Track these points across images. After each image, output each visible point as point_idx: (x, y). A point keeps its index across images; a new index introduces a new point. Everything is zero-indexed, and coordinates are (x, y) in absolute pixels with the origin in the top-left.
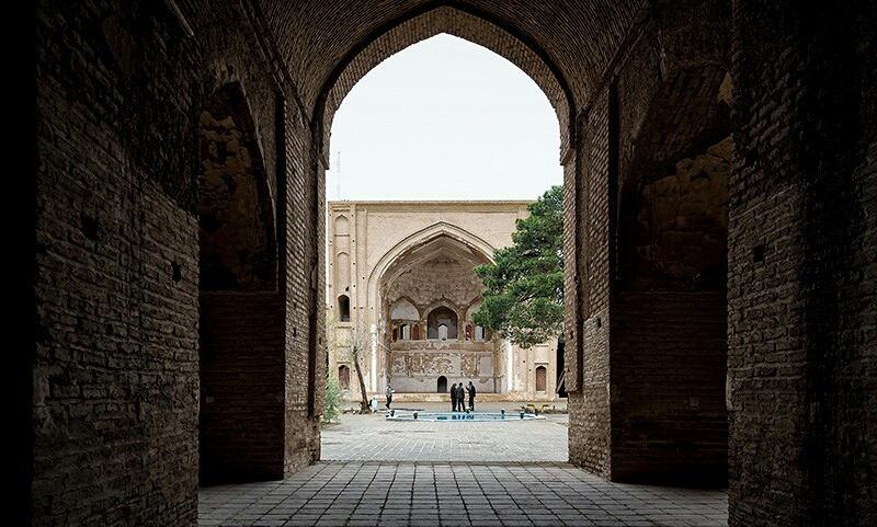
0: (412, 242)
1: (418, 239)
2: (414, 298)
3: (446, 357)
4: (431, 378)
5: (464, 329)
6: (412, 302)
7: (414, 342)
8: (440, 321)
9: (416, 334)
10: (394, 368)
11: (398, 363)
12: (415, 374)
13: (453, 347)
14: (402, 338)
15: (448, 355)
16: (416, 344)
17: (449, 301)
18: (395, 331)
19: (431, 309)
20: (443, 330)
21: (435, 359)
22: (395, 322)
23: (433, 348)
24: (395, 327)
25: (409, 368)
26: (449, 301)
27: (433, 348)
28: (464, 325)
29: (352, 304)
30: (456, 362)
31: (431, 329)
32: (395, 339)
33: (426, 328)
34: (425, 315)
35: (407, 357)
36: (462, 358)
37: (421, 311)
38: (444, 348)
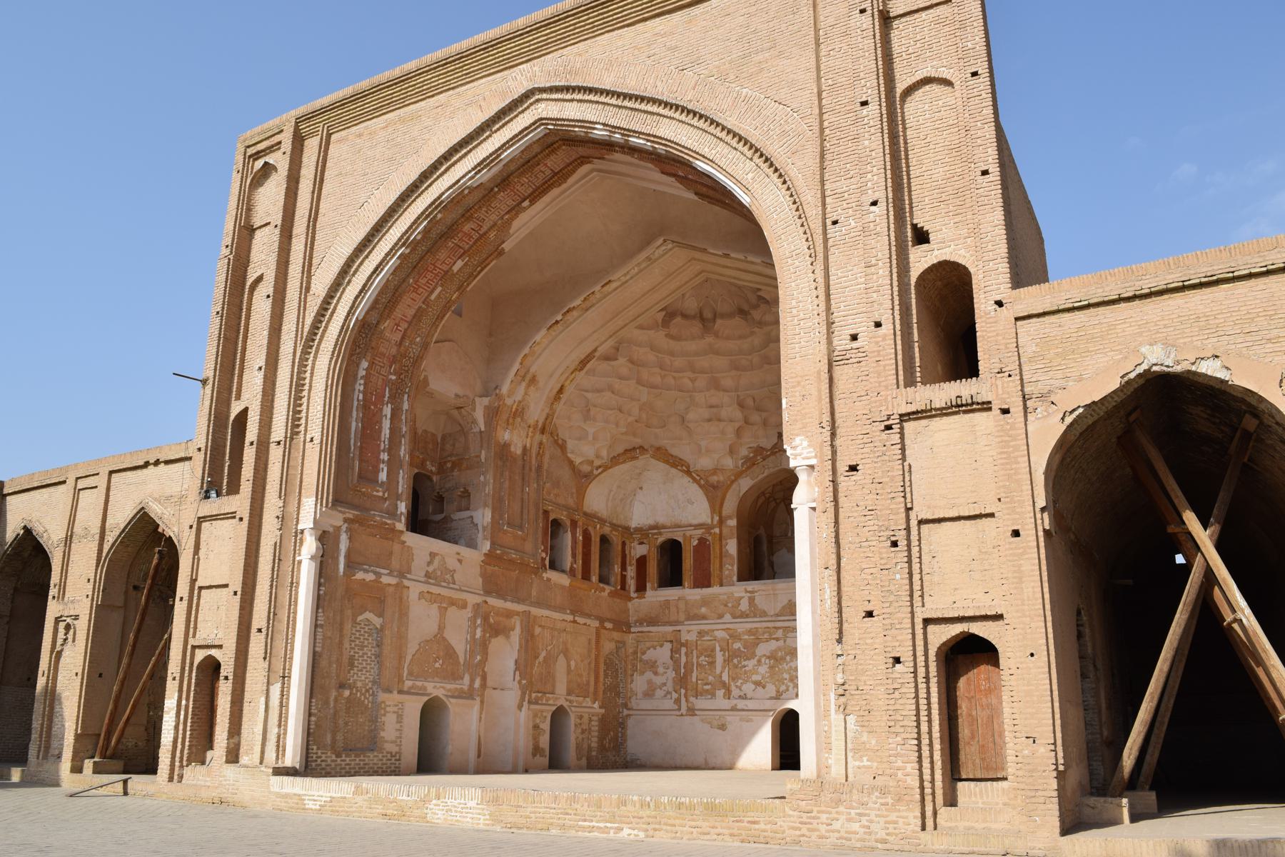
10: (639, 683)
11: (652, 666)
12: (700, 703)
16: (705, 602)
18: (642, 562)
19: (745, 484)
21: (763, 649)
22: (644, 534)
23: (754, 611)
24: (639, 550)
25: (682, 681)
27: (754, 611)
29: (252, 433)
32: (641, 588)
33: (732, 547)
34: (730, 505)
37: (714, 492)
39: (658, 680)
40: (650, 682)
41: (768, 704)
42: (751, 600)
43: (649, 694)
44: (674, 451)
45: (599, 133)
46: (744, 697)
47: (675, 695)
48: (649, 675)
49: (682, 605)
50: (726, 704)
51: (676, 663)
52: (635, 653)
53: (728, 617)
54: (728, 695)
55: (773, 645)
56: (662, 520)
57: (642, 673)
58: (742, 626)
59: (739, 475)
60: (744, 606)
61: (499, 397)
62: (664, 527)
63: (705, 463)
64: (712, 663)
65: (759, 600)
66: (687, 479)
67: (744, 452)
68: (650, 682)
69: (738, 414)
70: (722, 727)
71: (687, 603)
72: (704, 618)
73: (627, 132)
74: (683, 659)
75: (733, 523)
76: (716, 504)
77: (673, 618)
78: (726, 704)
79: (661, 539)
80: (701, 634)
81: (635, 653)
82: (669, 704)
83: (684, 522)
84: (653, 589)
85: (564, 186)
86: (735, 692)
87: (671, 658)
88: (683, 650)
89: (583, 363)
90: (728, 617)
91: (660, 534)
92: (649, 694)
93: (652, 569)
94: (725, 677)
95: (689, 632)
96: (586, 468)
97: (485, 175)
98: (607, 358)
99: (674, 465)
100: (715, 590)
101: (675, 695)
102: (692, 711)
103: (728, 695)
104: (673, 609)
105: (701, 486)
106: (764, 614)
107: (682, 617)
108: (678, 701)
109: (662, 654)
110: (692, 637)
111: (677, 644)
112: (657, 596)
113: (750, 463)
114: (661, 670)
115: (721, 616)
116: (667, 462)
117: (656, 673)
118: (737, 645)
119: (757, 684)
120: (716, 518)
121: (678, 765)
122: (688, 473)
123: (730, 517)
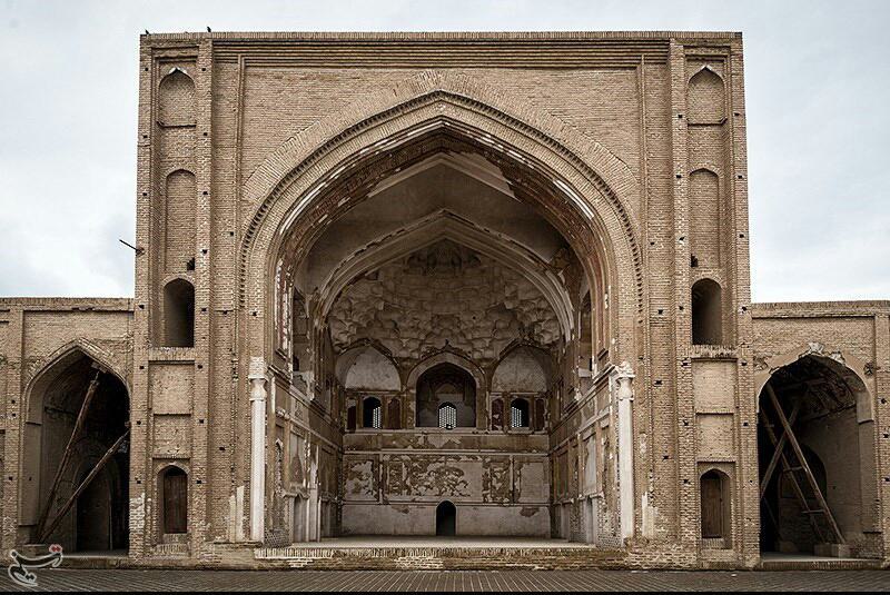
0: (361, 144)
1: (378, 138)
2: (392, 346)
3: (452, 463)
4: (421, 505)
5: (489, 408)
6: (385, 351)
7: (389, 433)
8: (444, 398)
9: (395, 420)
10: (350, 485)
11: (359, 475)
12: (391, 497)
13: (468, 444)
14: (368, 423)
15: (457, 458)
17: (458, 353)
18: (352, 411)
19: (422, 369)
20: (447, 415)
21: (431, 467)
22: (354, 393)
24: (351, 403)
25: (380, 485)
26: (458, 353)
27: (427, 445)
28: (489, 400)
30: (474, 473)
31: (426, 413)
32: (352, 427)
33: (413, 405)
34: (413, 380)
35: (376, 463)
36: (486, 465)
37: (403, 372)
38: (450, 445)
39: (362, 483)
40: (356, 484)
41: (435, 499)
42: (426, 439)
43: (357, 491)
44: (384, 343)
45: (487, 140)
46: (420, 494)
47: (375, 493)
48: (356, 480)
49: (380, 439)
50: (408, 498)
51: (376, 475)
52: (347, 466)
53: (410, 448)
54: (409, 493)
55: (439, 465)
56: (367, 385)
57: (351, 479)
58: (419, 453)
59: (419, 362)
60: (421, 441)
61: (319, 296)
62: (368, 390)
63: (404, 354)
64: (400, 474)
65: (429, 439)
66: (388, 361)
67: (424, 349)
68: (356, 484)
69: (429, 328)
70: (406, 511)
71: (383, 437)
72: (395, 447)
73: (508, 146)
74: (381, 472)
75: (414, 391)
76: (403, 382)
77: (373, 447)
78: (408, 498)
79: (366, 397)
80: (392, 456)
81: (347, 466)
82: (371, 497)
83: (382, 388)
84: (360, 428)
85: (420, 163)
86: (414, 491)
87: (372, 470)
88: (381, 466)
89: (357, 279)
90: (410, 448)
91: (366, 394)
92: (357, 491)
93: (360, 415)
94: (408, 483)
95: (385, 456)
96: (337, 349)
97: (394, 144)
98: (368, 278)
99: (383, 353)
100: (403, 431)
101: (375, 493)
102: (386, 502)
103: (409, 493)
104: (374, 441)
105: (397, 368)
106: (433, 447)
107: (380, 446)
108: (377, 496)
109: (366, 468)
110: (387, 458)
111: (376, 463)
112: (361, 433)
113: (427, 356)
114: (364, 477)
115: (406, 447)
116: (379, 349)
117: (361, 479)
118: (415, 464)
119: (428, 487)
120: (405, 388)
121: (376, 531)
122: (391, 358)
123: (412, 388)
